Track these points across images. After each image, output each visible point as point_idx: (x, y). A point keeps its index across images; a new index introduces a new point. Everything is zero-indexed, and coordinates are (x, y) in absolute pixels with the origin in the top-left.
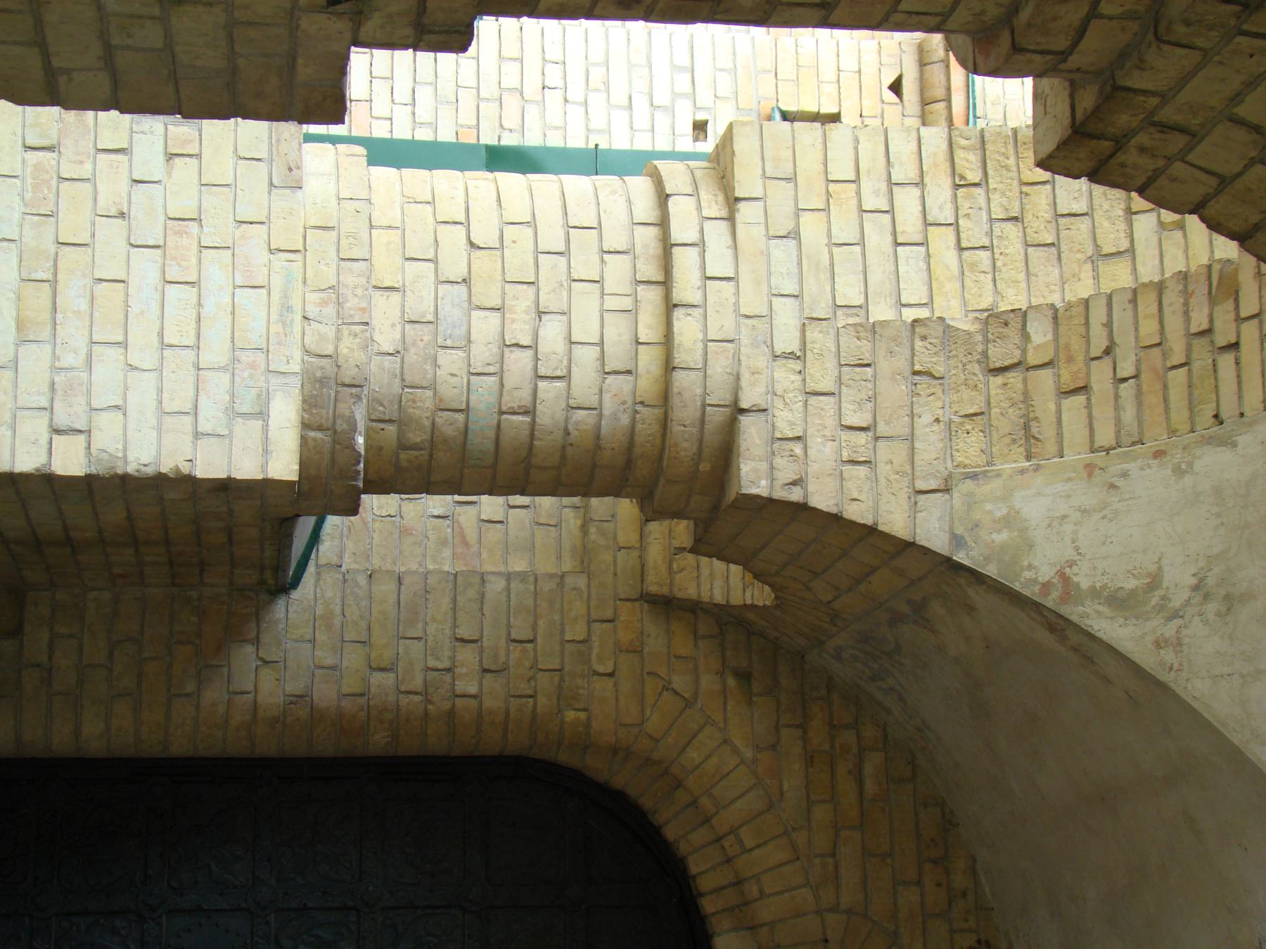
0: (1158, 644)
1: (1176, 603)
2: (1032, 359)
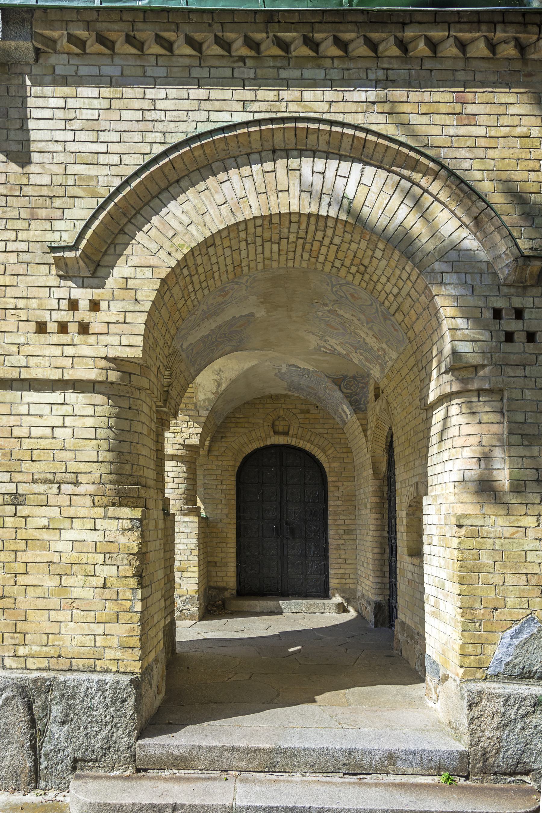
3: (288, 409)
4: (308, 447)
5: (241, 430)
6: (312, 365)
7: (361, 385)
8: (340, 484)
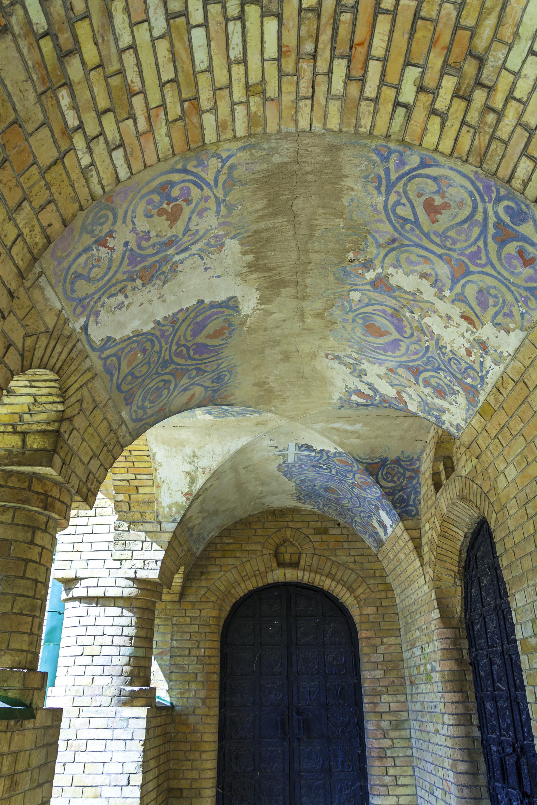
0: (204, 473)
1: (194, 468)
2: (128, 500)
3: (297, 529)
4: (327, 584)
5: (230, 561)
6: (334, 442)
7: (408, 474)
8: (377, 641)
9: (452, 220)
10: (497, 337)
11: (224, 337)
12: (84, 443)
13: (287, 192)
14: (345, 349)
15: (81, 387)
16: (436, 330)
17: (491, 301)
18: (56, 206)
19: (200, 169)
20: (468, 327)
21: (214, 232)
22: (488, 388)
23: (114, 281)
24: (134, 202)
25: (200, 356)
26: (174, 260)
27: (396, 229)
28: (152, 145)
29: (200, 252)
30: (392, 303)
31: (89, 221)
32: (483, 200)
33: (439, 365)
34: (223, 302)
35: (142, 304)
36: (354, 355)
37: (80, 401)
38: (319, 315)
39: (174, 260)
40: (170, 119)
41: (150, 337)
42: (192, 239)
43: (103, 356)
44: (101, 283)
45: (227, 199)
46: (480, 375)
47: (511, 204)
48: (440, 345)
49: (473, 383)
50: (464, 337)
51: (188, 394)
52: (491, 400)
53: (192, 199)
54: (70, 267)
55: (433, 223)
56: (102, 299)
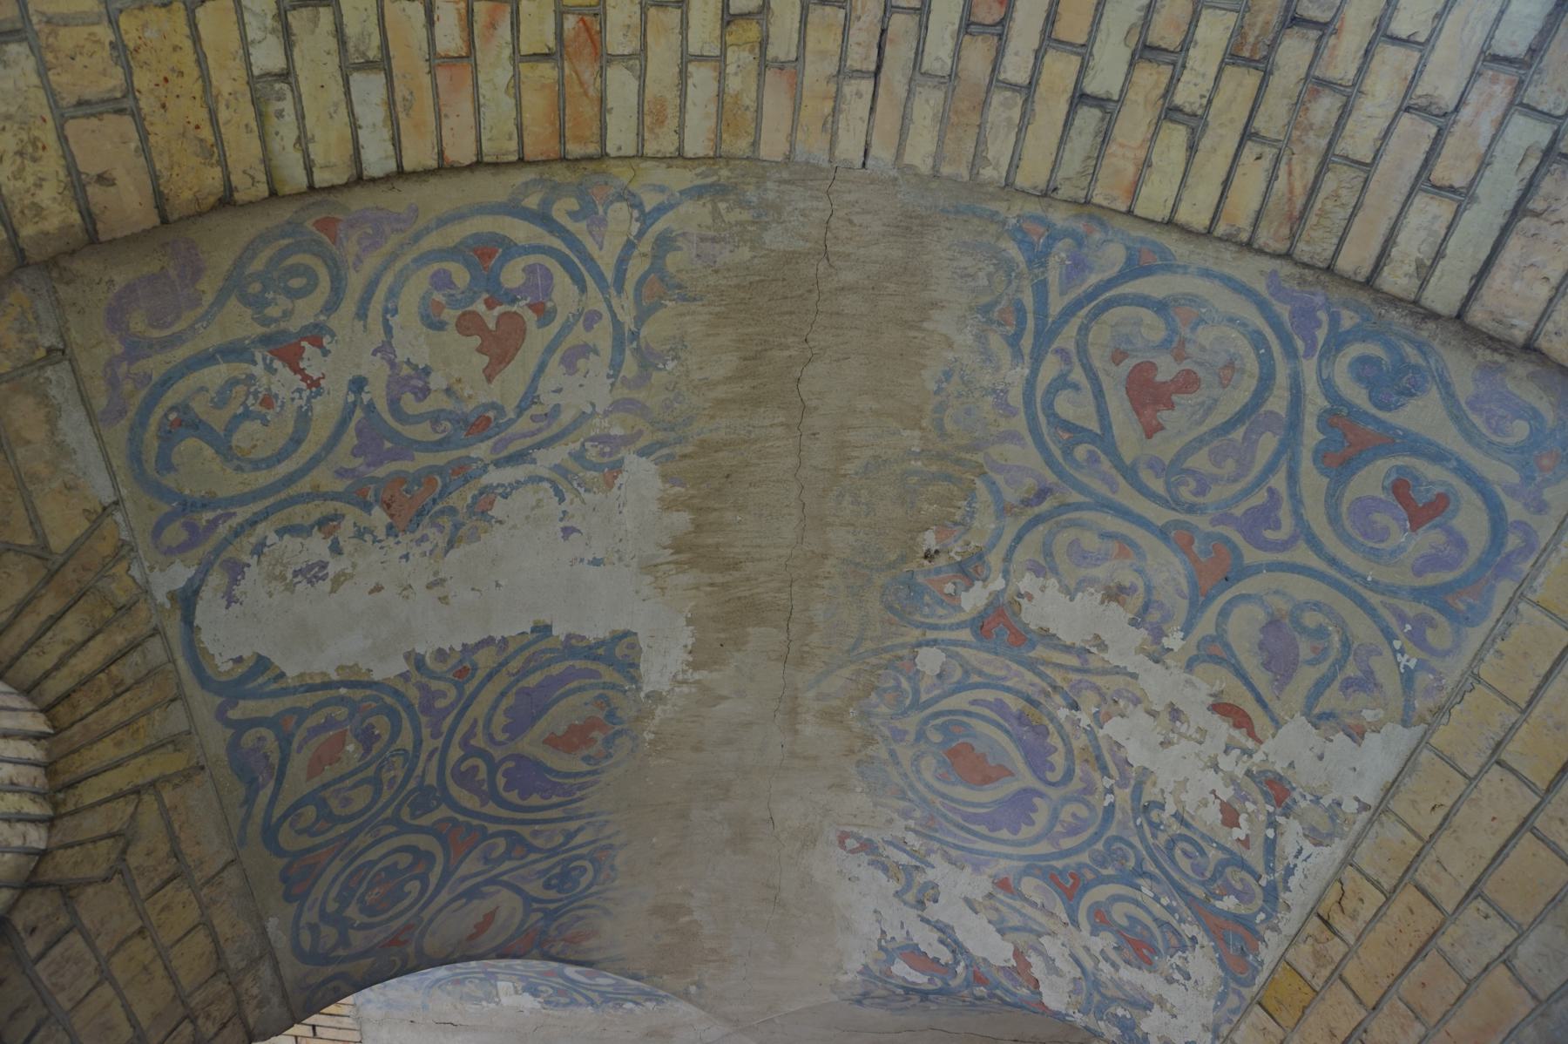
9: (1200, 423)
10: (1321, 758)
11: (592, 751)
12: (107, 991)
13: (791, 340)
14: (891, 821)
15: (137, 791)
16: (1137, 755)
17: (1305, 649)
18: (144, 136)
19: (583, 225)
20: (1231, 738)
21: (598, 425)
22: (1289, 922)
23: (304, 486)
24: (398, 265)
25: (523, 796)
26: (486, 480)
27: (1050, 462)
28: (467, 107)
29: (555, 476)
30: (1026, 680)
31: (258, 265)
32: (1290, 353)
33: (1140, 862)
34: (601, 643)
35: (378, 589)
36: (911, 838)
37: (123, 838)
38: (831, 717)
39: (486, 480)
40: (525, 49)
41: (389, 700)
42: (540, 430)
43: (234, 714)
44: (263, 478)
45: (644, 332)
46: (1263, 882)
47: (1374, 349)
48: (1144, 800)
49: (1243, 910)
50: (1216, 768)
51: (480, 907)
52: (1302, 957)
53: (554, 310)
54: (167, 382)
55: (1149, 436)
56: (261, 528)
